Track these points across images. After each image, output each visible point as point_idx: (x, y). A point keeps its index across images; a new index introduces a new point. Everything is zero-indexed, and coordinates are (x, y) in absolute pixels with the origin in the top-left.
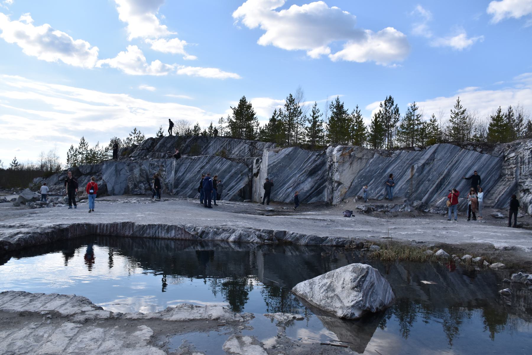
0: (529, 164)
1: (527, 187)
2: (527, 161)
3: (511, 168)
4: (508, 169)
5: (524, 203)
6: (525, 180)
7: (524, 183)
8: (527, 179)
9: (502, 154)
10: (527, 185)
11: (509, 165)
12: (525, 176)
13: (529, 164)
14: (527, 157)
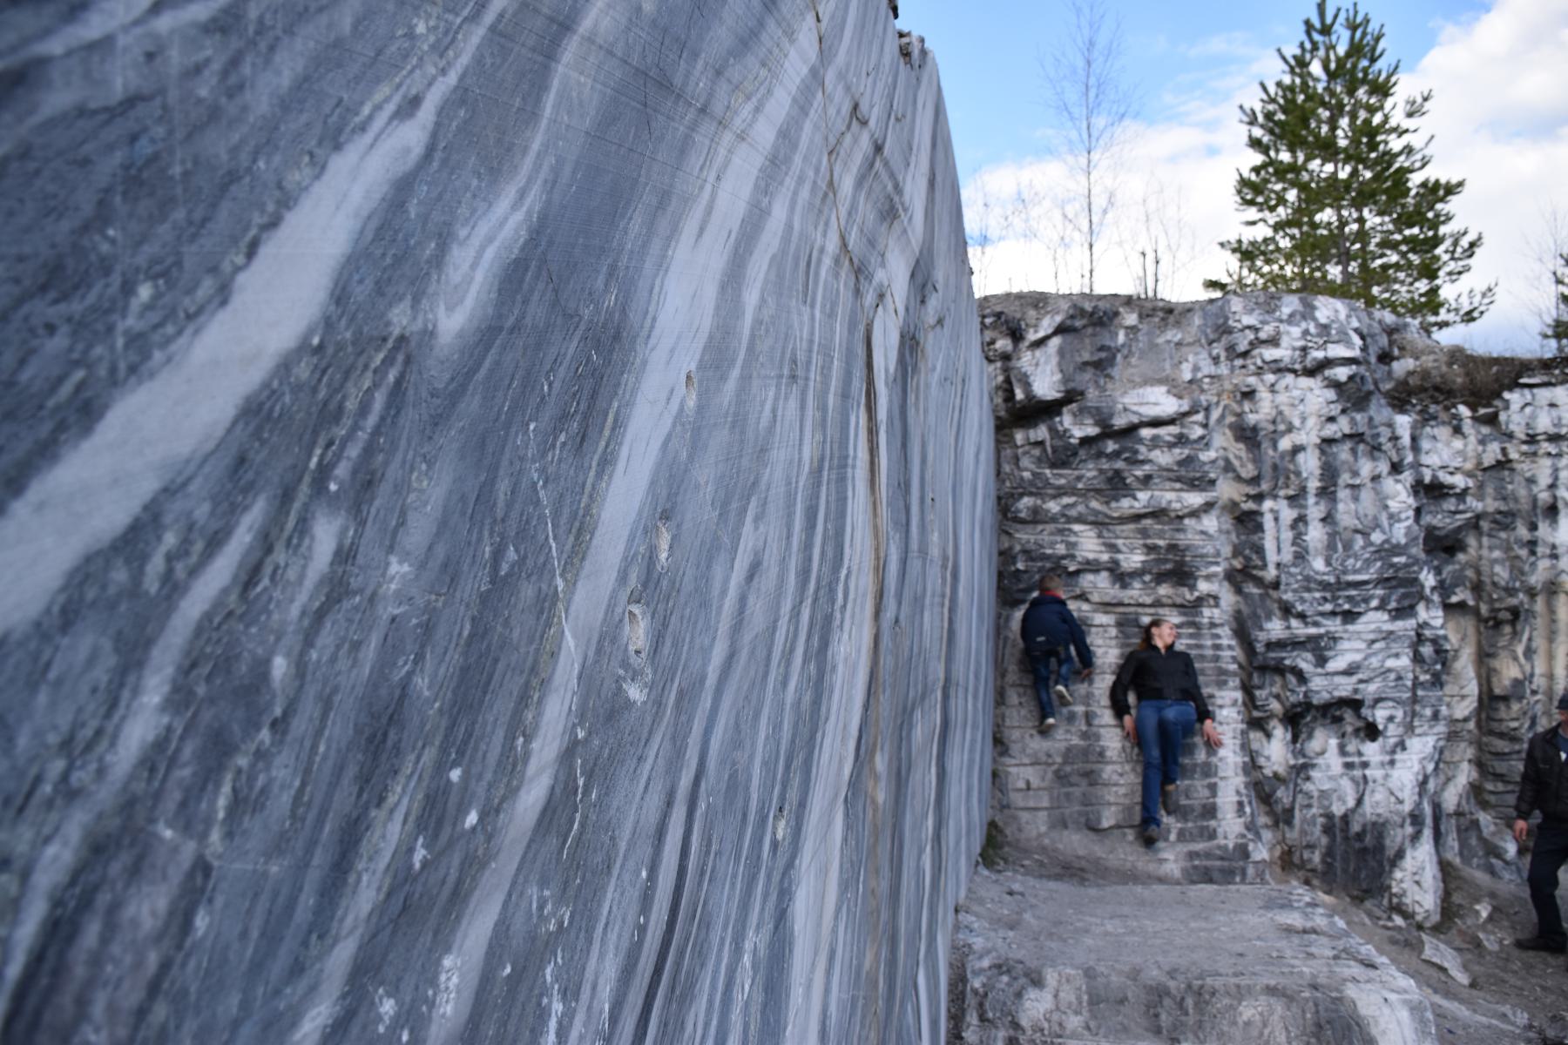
0: (1327, 492)
2: (1310, 464)
3: (1159, 514)
4: (1100, 523)
5: (1336, 827)
6: (1334, 625)
7: (1320, 649)
8: (1350, 617)
10: (1349, 672)
11: (1116, 485)
12: (1332, 589)
13: (1327, 492)
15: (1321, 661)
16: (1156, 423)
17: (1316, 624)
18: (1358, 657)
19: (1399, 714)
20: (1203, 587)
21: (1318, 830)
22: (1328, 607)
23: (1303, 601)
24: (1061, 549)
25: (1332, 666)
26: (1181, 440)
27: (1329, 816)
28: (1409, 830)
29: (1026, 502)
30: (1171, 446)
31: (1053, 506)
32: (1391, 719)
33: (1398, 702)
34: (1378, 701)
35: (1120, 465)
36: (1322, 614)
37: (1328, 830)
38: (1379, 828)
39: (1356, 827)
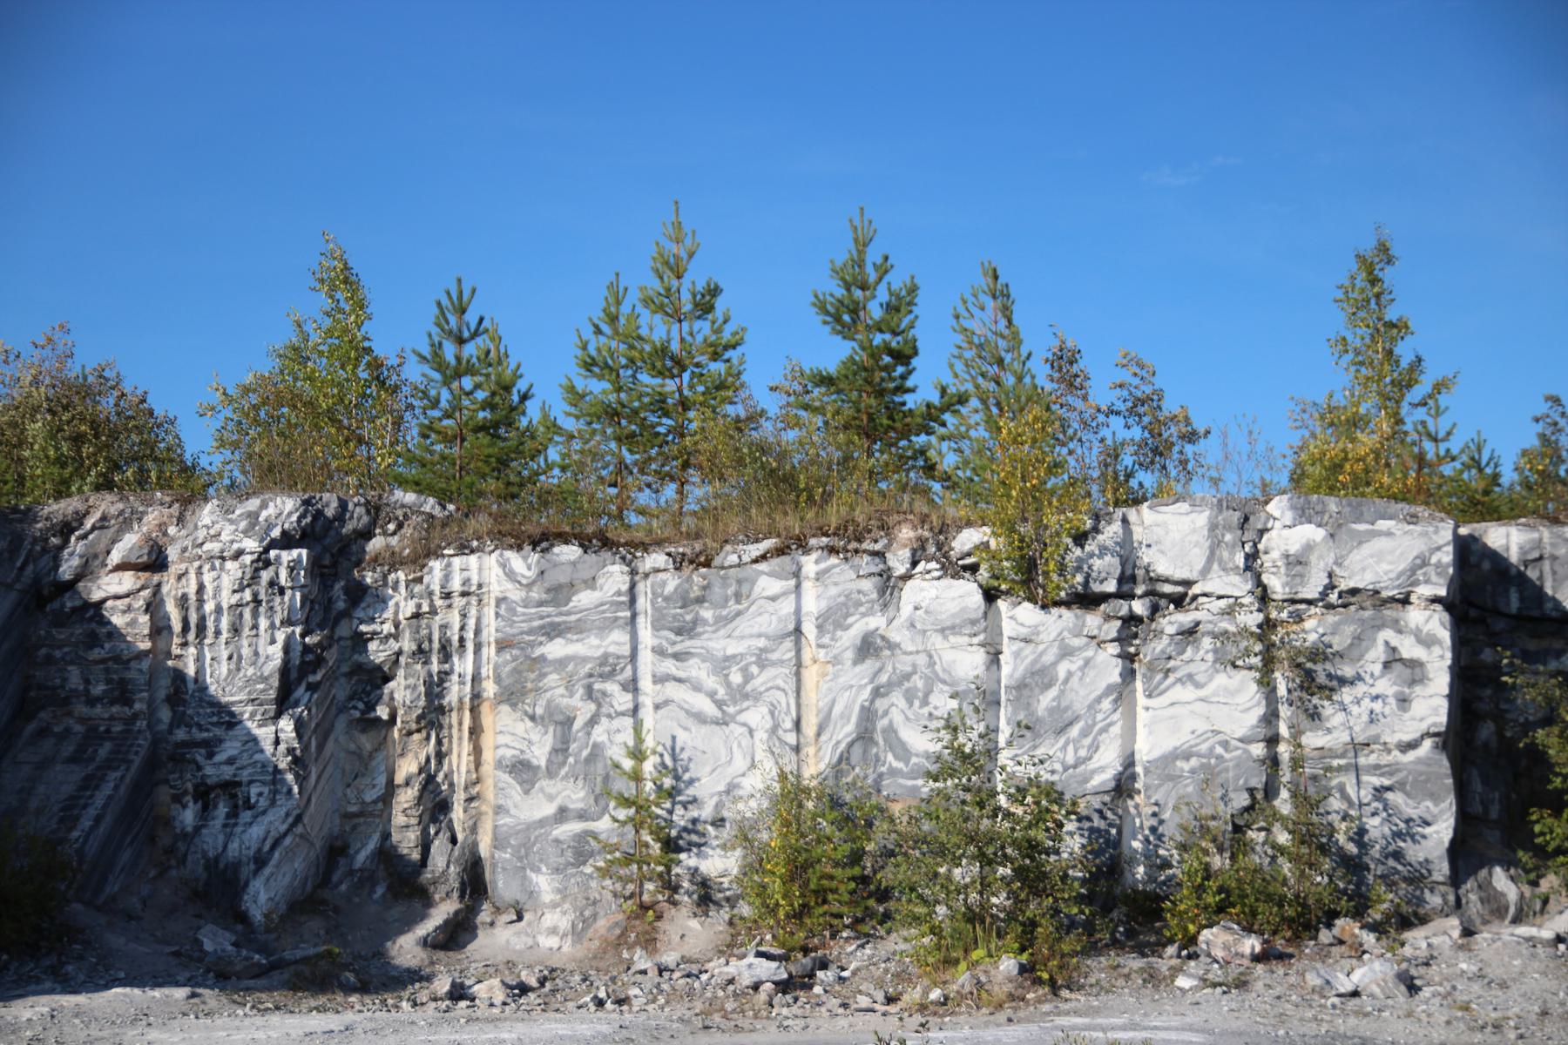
1: (227, 772)
5: (212, 864)
6: (218, 731)
9: (30, 568)
10: (230, 761)
14: (227, 599)
15: (211, 755)
16: (117, 597)
17: (207, 730)
18: (235, 752)
19: (266, 790)
20: (137, 706)
21: (201, 869)
22: (215, 719)
23: (198, 714)
24: (58, 681)
25: (218, 758)
26: (129, 609)
27: (208, 860)
28: (252, 867)
29: (43, 651)
30: (124, 612)
31: (58, 654)
32: (260, 794)
33: (264, 783)
34: (250, 782)
35: (94, 625)
36: (212, 724)
37: (207, 868)
38: (236, 866)
39: (221, 866)
